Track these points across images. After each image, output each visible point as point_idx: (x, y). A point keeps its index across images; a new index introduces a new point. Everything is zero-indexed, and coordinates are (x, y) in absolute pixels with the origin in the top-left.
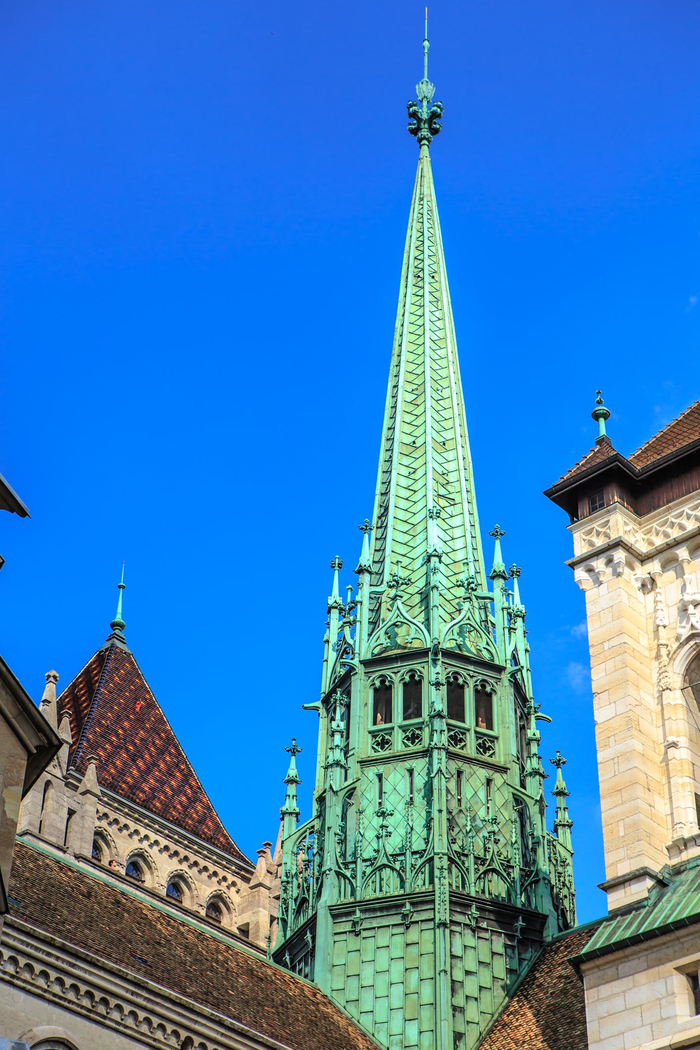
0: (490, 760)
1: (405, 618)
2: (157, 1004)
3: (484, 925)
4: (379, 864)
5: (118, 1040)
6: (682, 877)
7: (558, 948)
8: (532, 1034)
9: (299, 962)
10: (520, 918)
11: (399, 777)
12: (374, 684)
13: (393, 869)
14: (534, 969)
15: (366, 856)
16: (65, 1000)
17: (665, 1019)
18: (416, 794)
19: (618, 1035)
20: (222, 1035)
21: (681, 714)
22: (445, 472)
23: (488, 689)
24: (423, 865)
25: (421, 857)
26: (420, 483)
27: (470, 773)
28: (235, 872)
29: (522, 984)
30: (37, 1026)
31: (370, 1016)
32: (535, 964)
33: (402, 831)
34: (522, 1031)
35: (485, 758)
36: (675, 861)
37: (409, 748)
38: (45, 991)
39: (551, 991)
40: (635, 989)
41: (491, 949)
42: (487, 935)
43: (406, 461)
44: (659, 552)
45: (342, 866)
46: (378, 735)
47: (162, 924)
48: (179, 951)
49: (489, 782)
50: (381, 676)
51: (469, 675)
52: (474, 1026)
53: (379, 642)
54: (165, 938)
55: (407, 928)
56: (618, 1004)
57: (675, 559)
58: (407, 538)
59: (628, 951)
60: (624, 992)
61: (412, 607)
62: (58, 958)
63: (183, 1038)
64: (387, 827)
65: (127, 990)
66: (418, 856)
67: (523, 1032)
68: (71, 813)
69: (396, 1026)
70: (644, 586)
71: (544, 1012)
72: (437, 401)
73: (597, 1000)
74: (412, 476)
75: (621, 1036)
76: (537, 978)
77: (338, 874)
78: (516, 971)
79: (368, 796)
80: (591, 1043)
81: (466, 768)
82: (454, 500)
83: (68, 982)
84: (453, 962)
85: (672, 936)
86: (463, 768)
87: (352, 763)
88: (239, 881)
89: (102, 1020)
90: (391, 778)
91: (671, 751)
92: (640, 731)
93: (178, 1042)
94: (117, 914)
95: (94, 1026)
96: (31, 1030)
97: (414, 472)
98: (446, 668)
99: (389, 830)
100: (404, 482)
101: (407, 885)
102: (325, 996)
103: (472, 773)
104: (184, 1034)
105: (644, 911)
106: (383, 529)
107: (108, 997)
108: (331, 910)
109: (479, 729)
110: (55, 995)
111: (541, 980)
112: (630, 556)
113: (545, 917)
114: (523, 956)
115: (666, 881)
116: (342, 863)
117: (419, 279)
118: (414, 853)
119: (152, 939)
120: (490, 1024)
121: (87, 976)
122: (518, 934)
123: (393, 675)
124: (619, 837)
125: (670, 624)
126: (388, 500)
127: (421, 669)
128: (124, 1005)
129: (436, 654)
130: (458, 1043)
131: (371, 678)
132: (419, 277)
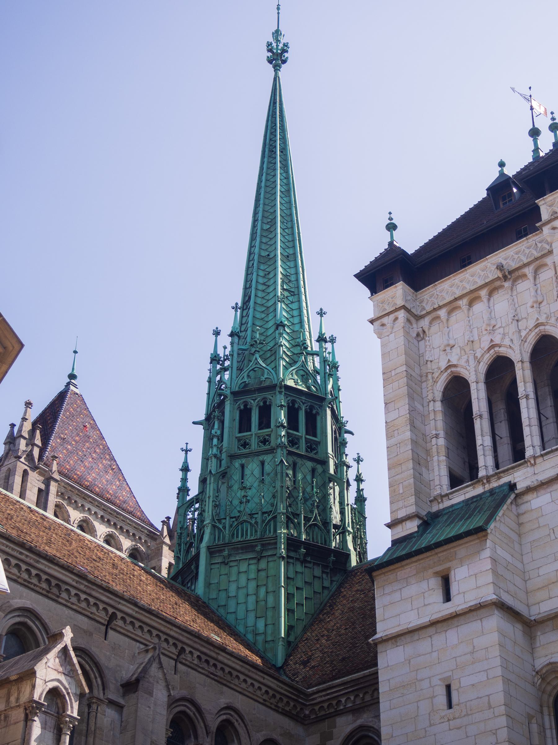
0: (314, 456)
1: (261, 365)
2: (94, 590)
3: (309, 559)
4: (241, 520)
5: (67, 612)
6: (440, 519)
7: (356, 573)
8: (338, 625)
9: (188, 583)
10: (332, 555)
11: (255, 465)
12: (240, 407)
13: (251, 524)
14: (340, 586)
15: (232, 516)
16: (32, 583)
17: (427, 605)
18: (265, 477)
19: (396, 616)
20: (137, 612)
21: (440, 417)
22: (288, 274)
23: (314, 412)
24: (270, 520)
25: (269, 515)
26: (272, 281)
27: (301, 464)
28: (146, 534)
29: (332, 596)
30: (13, 599)
31: (233, 615)
32: (340, 584)
33: (256, 500)
34: (332, 624)
35: (311, 455)
36: (435, 508)
37: (263, 448)
38: (19, 577)
39: (351, 599)
40: (407, 587)
41: (313, 574)
42: (311, 565)
43: (262, 267)
44: (428, 313)
45: (216, 521)
46: (242, 440)
47: (98, 550)
48: (109, 567)
49: (313, 471)
50: (244, 402)
51: (302, 402)
52: (301, 621)
53: (243, 381)
54: (100, 558)
55: (259, 560)
56: (397, 596)
57: (438, 317)
58: (263, 315)
59: (404, 563)
60: (400, 589)
61: (265, 359)
62: (27, 556)
63: (110, 613)
64: (247, 496)
65: (74, 580)
66: (267, 515)
67: (333, 624)
68: (40, 490)
69: (251, 621)
70: (418, 335)
71: (346, 612)
72: (283, 229)
73: (383, 595)
74: (267, 276)
75: (398, 616)
76: (342, 592)
77: (214, 527)
78: (329, 588)
79: (235, 478)
80: (378, 622)
81: (299, 461)
82: (293, 292)
83: (34, 572)
84: (288, 582)
85: (433, 552)
86: (297, 461)
87: (224, 456)
88: (149, 540)
89: (56, 598)
90: (250, 467)
91: (434, 440)
92: (414, 427)
93: (106, 615)
94: (68, 541)
95: (51, 602)
96: (9, 602)
97: (268, 274)
98: (287, 397)
99: (248, 498)
100: (261, 280)
101: (259, 533)
102: (204, 603)
103: (303, 464)
104: (111, 610)
105: (414, 540)
106: (247, 310)
107: (60, 584)
108: (209, 549)
109: (308, 437)
110: (25, 580)
111: (345, 593)
112: (409, 315)
113: (348, 556)
114: (334, 579)
115: (429, 521)
116: (217, 519)
117: (273, 153)
118: (264, 513)
119: (91, 558)
120: (311, 621)
121: (47, 569)
122: (331, 565)
123: (252, 401)
124: (399, 494)
125: (435, 360)
126: (251, 292)
127: (271, 398)
128: (71, 589)
129: (281, 388)
130: (290, 632)
131: (238, 403)
132: (273, 151)
